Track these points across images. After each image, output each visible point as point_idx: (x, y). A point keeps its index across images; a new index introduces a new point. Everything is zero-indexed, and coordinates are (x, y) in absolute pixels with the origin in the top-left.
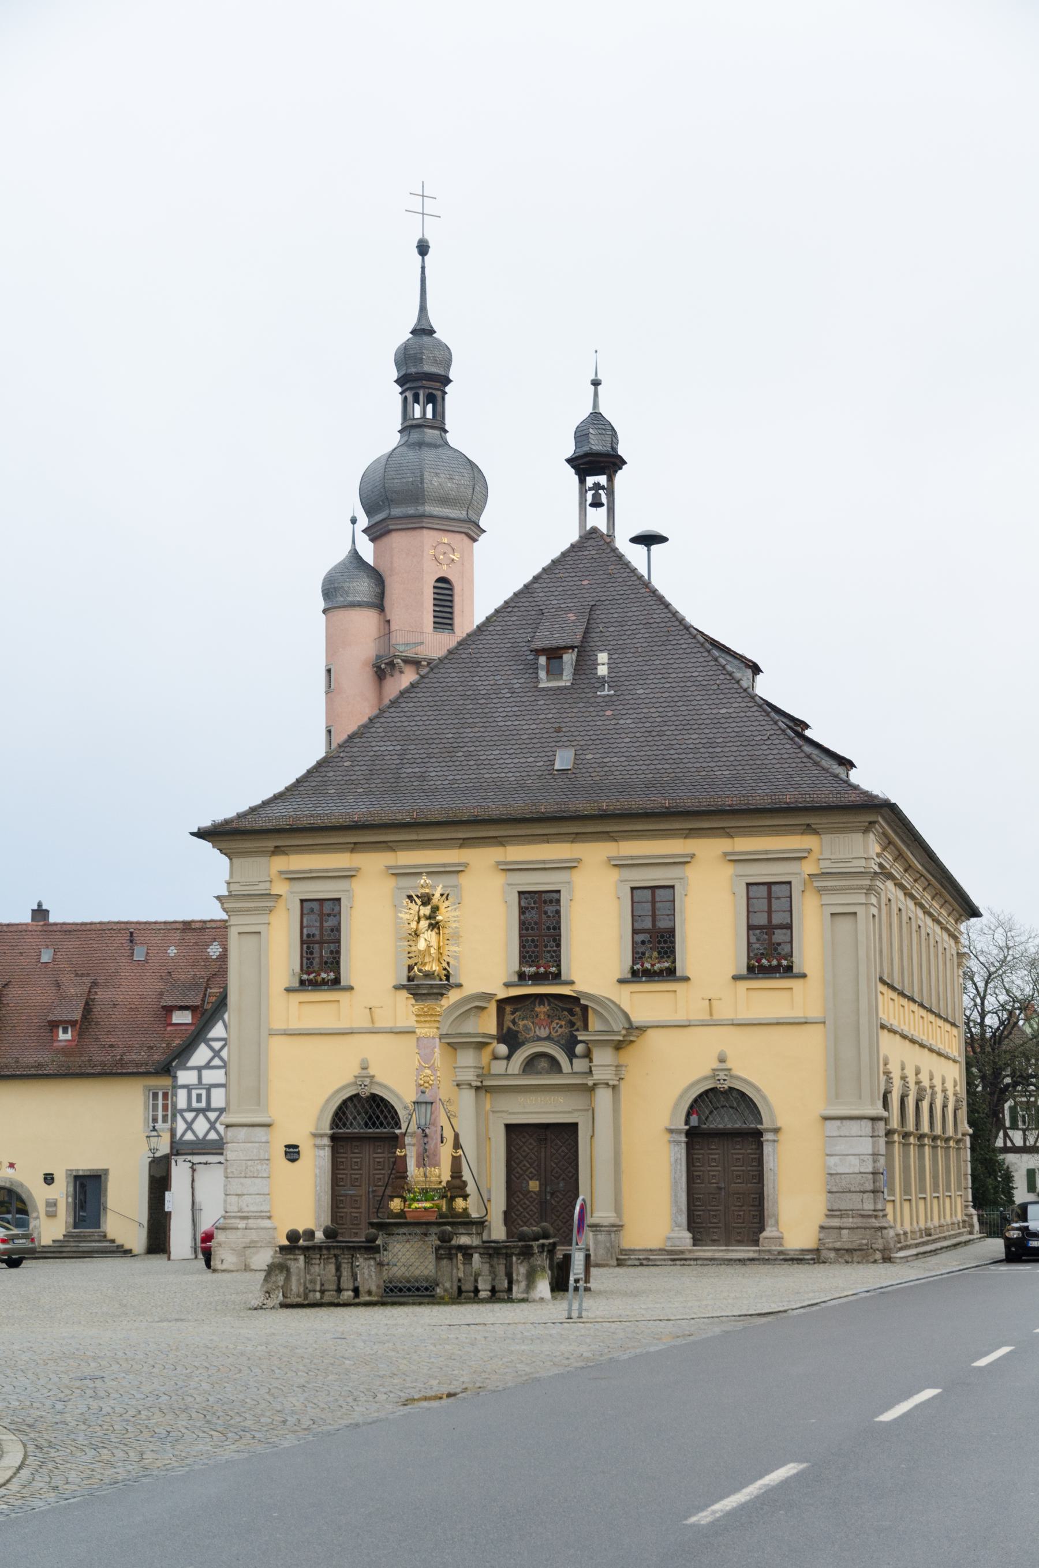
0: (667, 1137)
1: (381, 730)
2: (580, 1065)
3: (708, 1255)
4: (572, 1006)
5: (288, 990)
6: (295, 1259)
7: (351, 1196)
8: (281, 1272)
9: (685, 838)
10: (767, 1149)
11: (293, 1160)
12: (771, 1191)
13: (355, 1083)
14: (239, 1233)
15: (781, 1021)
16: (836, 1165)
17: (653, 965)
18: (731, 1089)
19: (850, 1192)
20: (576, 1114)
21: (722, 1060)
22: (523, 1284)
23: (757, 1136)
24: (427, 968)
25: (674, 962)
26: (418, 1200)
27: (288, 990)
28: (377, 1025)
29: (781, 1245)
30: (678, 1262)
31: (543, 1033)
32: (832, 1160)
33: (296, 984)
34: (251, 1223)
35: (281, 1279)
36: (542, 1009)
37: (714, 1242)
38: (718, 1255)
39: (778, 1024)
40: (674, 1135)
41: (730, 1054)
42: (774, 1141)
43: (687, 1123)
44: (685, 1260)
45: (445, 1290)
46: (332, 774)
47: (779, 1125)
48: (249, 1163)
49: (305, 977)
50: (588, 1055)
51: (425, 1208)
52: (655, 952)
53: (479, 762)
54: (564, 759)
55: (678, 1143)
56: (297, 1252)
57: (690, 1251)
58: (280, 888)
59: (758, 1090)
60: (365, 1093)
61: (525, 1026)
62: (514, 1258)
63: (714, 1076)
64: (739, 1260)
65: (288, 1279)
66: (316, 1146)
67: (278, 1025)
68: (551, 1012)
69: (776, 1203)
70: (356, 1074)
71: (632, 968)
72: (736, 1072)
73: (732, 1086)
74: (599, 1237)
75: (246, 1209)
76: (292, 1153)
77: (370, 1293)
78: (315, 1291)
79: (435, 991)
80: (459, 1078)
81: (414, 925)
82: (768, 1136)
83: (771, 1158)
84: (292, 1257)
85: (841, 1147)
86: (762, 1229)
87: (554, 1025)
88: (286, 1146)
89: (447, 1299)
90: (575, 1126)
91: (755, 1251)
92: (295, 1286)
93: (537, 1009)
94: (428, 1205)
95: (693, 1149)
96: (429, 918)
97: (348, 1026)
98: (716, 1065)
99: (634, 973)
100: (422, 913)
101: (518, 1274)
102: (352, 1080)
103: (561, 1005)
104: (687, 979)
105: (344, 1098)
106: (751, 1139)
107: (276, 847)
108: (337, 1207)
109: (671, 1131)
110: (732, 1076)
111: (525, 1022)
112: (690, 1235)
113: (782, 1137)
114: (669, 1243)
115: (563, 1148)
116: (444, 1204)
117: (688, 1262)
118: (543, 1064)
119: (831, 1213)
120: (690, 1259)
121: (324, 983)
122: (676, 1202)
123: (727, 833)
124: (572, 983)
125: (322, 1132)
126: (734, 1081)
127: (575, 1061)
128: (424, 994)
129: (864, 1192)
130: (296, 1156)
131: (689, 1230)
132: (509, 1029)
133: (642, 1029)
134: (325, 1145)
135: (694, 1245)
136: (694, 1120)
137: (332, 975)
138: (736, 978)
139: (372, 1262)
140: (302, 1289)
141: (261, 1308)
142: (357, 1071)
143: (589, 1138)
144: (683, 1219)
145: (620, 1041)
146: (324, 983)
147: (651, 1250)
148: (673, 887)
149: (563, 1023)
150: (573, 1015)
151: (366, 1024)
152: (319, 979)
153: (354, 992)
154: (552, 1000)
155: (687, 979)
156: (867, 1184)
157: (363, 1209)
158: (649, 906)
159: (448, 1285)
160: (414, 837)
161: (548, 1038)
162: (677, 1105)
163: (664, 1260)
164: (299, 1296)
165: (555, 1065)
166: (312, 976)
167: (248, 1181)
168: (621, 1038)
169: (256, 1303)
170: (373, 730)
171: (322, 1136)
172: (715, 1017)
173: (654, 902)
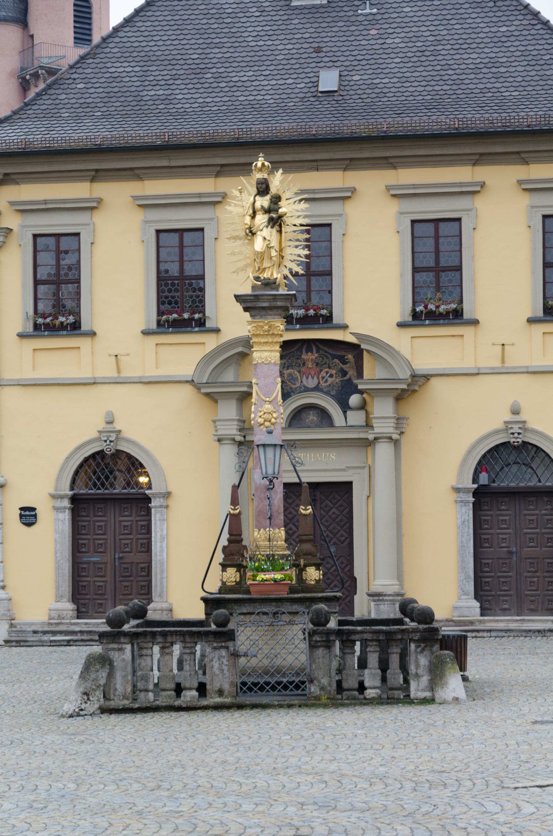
0: (454, 496)
1: (116, 50)
2: (356, 418)
3: (501, 626)
4: (343, 353)
5: (21, 336)
6: (120, 649)
7: (95, 563)
8: (103, 666)
9: (474, 165)
11: (29, 525)
13: (98, 439)
17: (438, 307)
20: (350, 472)
21: (516, 412)
22: (425, 680)
24: (266, 275)
25: (461, 301)
26: (263, 571)
27: (21, 336)
28: (123, 375)
31: (311, 383)
33: (30, 328)
35: (103, 675)
36: (310, 357)
37: (505, 611)
38: (513, 626)
40: (461, 495)
41: (524, 405)
43: (475, 481)
44: (478, 631)
45: (322, 688)
46: (64, 96)
49: (40, 321)
50: (363, 406)
51: (275, 581)
52: (438, 292)
53: (232, 84)
54: (329, 80)
55: (465, 503)
56: (122, 640)
57: (480, 622)
58: (12, 221)
60: (109, 449)
61: (290, 375)
62: (413, 646)
63: (507, 429)
64: (539, 631)
65: (110, 676)
66: (56, 509)
67: (9, 375)
70: (100, 429)
71: (414, 310)
72: (531, 425)
73: (526, 440)
74: (382, 607)
76: (28, 516)
77: (220, 692)
78: (147, 691)
79: (279, 304)
80: (220, 432)
81: (248, 220)
84: (115, 646)
87: (323, 374)
88: (21, 509)
89: (324, 700)
90: (349, 485)
92: (121, 685)
93: (304, 356)
94: (278, 576)
95: (481, 510)
96: (267, 211)
97: (90, 375)
98: (509, 417)
99: (416, 315)
100: (258, 205)
101: (417, 666)
102: (95, 435)
103: (330, 351)
104: (475, 322)
105: (87, 455)
106: (546, 499)
107: (6, 175)
108: (79, 576)
109: (457, 490)
110: (526, 430)
111: (290, 371)
112: (478, 604)
114: (456, 613)
115: (334, 510)
116: (293, 573)
117: (481, 634)
118: (312, 417)
120: (483, 631)
121: (63, 327)
122: (463, 568)
123: (522, 159)
124: (345, 327)
125: (62, 493)
126: (528, 435)
127: (349, 413)
128: (263, 308)
130: (32, 519)
131: (477, 597)
133: (427, 377)
134: (65, 508)
135: (482, 615)
136: (484, 478)
137: (71, 319)
138: (531, 321)
139: (224, 652)
140: (129, 689)
141: (79, 715)
142: (101, 426)
143: (365, 498)
145: (403, 390)
146: (63, 327)
148: (459, 220)
149: (334, 372)
150: (345, 363)
151: (111, 373)
152: (57, 322)
153: (96, 339)
154: (321, 347)
155: (475, 322)
157: (109, 577)
158: (432, 241)
159: (325, 681)
160: (165, 163)
161: (317, 389)
162: (464, 461)
164: (125, 697)
165: (325, 418)
166: (48, 320)
168: (404, 386)
169: (69, 707)
170: (108, 50)
171: (62, 497)
172: (506, 365)
173: (437, 237)
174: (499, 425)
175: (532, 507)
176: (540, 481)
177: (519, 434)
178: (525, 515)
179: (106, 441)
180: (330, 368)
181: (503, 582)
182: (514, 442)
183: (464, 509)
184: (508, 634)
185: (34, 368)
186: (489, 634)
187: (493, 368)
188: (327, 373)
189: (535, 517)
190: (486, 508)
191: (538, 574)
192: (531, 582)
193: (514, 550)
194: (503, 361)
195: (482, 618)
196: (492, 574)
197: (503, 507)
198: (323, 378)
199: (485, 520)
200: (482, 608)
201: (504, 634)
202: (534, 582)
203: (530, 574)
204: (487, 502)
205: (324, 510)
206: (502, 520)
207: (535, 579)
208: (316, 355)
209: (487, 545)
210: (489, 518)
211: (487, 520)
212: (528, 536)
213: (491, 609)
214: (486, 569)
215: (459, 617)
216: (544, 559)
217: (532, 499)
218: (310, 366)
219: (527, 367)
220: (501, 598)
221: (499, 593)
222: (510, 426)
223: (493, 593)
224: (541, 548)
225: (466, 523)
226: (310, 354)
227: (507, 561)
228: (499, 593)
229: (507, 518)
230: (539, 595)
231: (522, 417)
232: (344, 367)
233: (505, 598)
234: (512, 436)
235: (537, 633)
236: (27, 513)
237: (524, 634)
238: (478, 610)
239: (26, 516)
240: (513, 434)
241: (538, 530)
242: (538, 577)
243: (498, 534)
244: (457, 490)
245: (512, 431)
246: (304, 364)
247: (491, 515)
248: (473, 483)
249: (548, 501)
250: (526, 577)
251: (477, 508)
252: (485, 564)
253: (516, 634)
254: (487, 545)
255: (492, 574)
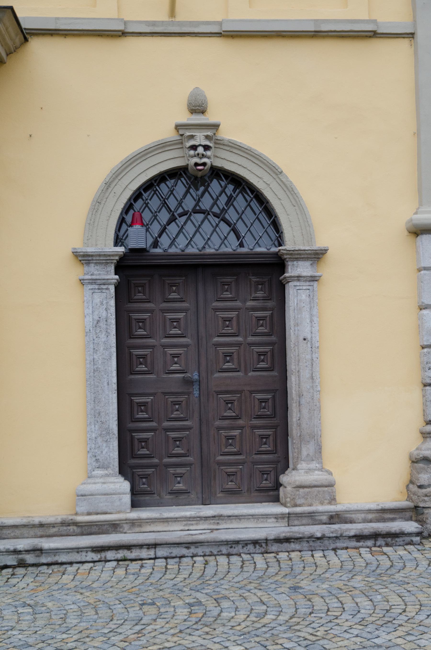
0: (78, 271)
3: (176, 533)
10: (296, 296)
12: (306, 385)
15: (324, 28)
18: (217, 173)
21: (197, 107)
23: (268, 273)
29: (333, 500)
30: (110, 555)
37: (179, 497)
38: (199, 532)
39: (316, 35)
40: (92, 268)
42: (314, 279)
43: (118, 241)
44: (129, 547)
47: (319, 245)
55: (99, 284)
57: (133, 523)
59: (275, 171)
64: (255, 542)
69: (316, 409)
73: (218, 163)
82: (294, 269)
83: (306, 315)
86: (283, 464)
91: (278, 517)
98: (185, 118)
106: (254, 279)
109: (84, 258)
110: (219, 143)
113: (327, 270)
114: (83, 507)
117: (134, 554)
120: (141, 546)
122: (96, 415)
126: (222, 153)
136: (137, 237)
144: (111, 452)
147: (41, 525)
162: (98, 203)
163: (78, 550)
172: (181, 17)
174: (166, 132)
175: (227, 295)
176: (241, 245)
177: (207, 148)
178: (216, 310)
181: (175, 440)
182: (196, 164)
183: (98, 297)
184: (193, 550)
186: (151, 553)
187: (154, 24)
189: (233, 314)
190: (140, 296)
191: (241, 422)
192: (228, 438)
193: (196, 376)
194: (172, 12)
195: (134, 515)
196: (154, 424)
197: (174, 296)
199: (138, 321)
200: (134, 492)
201: (184, 551)
202: (233, 438)
203: (226, 423)
204: (143, 286)
206: (172, 321)
207: (236, 433)
209: (143, 368)
210: (146, 316)
211: (143, 321)
212: (222, 350)
213: (151, 493)
214: (141, 415)
215: (89, 514)
216: (251, 392)
217: (228, 279)
219: (220, 23)
220: (172, 470)
221: (166, 460)
222: (188, 134)
223: (156, 461)
224: (246, 373)
225: (102, 324)
227: (182, 398)
228: (166, 460)
229: (181, 315)
230: (242, 463)
231: (210, 118)
233: (179, 470)
234: (192, 152)
235: (251, 547)
237: (224, 550)
238: (127, 499)
240: (194, 147)
241: (240, 339)
242: (241, 428)
243: (165, 346)
244: (84, 258)
245: (192, 143)
247: (151, 311)
248: (116, 244)
249: (258, 283)
250: (219, 429)
251: (123, 296)
252: (140, 405)
253: (207, 550)
254: (143, 368)
255: (154, 424)
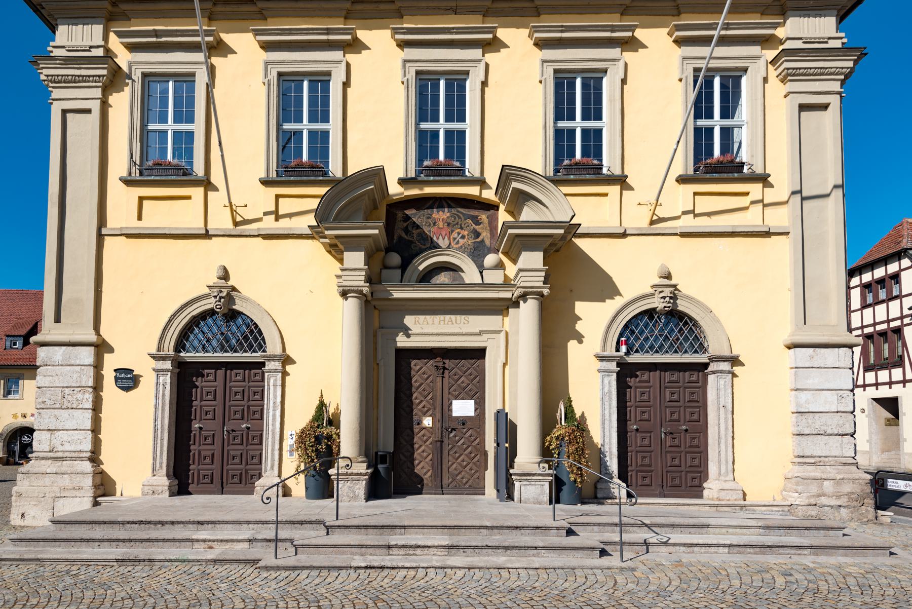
11: (127, 389)
14: (47, 480)
16: (807, 402)
19: (825, 434)
32: (803, 396)
34: (66, 466)
48: (67, 391)
68: (451, 220)
75: (60, 448)
85: (814, 379)
87: (455, 235)
88: (115, 370)
98: (658, 281)
105: (194, 313)
109: (601, 358)
119: (802, 459)
129: (842, 435)
132: (400, 237)
149: (466, 233)
150: (478, 223)
156: (847, 425)
167: (64, 414)
179: (215, 297)
180: (462, 228)
185: (140, 218)
188: (459, 234)
198: (455, 239)
205: (453, 379)
208: (448, 214)
218: (441, 226)
226: (441, 213)
231: (673, 282)
232: (477, 227)
236: (124, 375)
239: (122, 378)
240: (664, 298)
246: (434, 224)
